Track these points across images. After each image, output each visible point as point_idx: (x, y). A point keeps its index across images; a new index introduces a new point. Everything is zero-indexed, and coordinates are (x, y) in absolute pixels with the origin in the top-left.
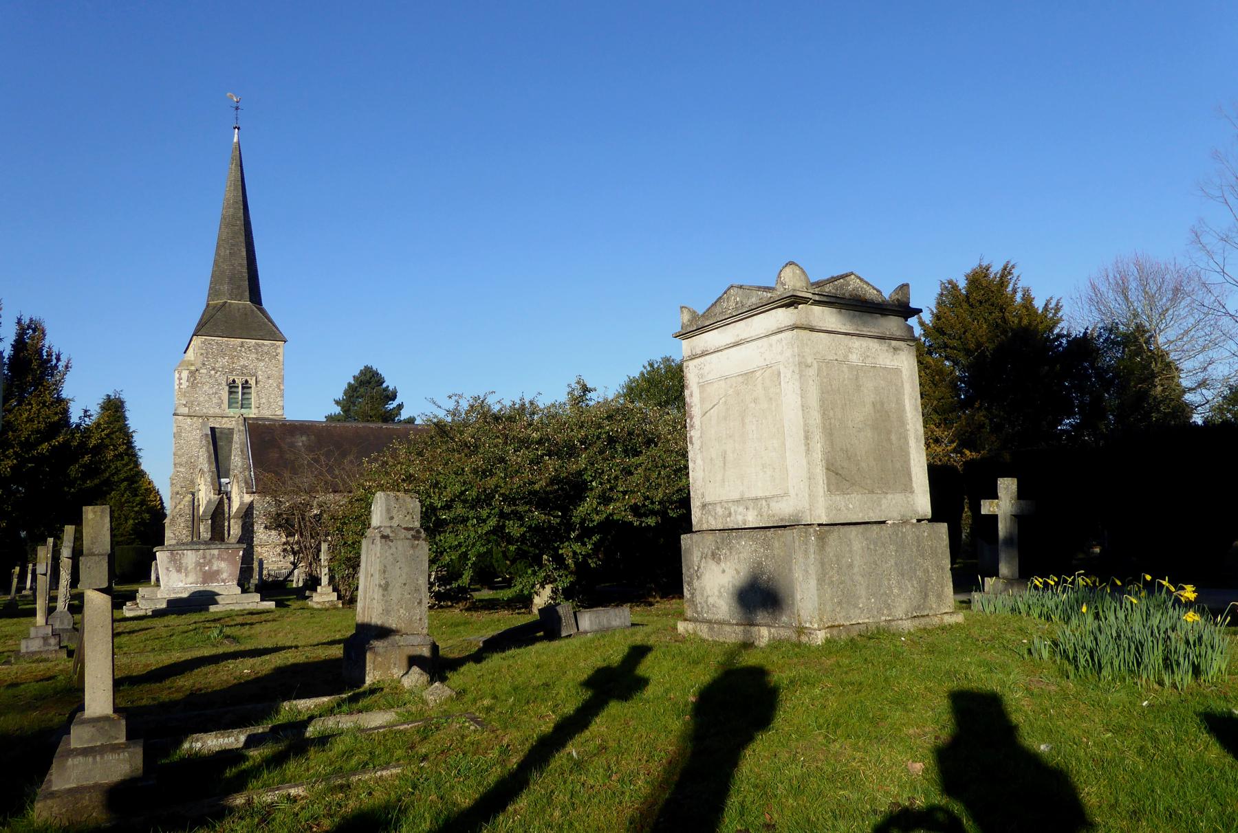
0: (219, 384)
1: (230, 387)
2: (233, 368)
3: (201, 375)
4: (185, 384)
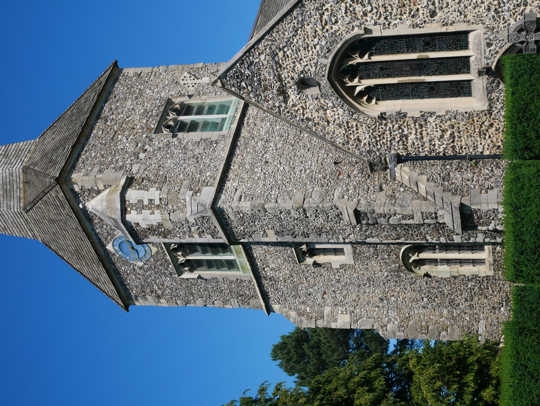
0: (168, 145)
2: (142, 128)
3: (141, 172)
4: (154, 194)
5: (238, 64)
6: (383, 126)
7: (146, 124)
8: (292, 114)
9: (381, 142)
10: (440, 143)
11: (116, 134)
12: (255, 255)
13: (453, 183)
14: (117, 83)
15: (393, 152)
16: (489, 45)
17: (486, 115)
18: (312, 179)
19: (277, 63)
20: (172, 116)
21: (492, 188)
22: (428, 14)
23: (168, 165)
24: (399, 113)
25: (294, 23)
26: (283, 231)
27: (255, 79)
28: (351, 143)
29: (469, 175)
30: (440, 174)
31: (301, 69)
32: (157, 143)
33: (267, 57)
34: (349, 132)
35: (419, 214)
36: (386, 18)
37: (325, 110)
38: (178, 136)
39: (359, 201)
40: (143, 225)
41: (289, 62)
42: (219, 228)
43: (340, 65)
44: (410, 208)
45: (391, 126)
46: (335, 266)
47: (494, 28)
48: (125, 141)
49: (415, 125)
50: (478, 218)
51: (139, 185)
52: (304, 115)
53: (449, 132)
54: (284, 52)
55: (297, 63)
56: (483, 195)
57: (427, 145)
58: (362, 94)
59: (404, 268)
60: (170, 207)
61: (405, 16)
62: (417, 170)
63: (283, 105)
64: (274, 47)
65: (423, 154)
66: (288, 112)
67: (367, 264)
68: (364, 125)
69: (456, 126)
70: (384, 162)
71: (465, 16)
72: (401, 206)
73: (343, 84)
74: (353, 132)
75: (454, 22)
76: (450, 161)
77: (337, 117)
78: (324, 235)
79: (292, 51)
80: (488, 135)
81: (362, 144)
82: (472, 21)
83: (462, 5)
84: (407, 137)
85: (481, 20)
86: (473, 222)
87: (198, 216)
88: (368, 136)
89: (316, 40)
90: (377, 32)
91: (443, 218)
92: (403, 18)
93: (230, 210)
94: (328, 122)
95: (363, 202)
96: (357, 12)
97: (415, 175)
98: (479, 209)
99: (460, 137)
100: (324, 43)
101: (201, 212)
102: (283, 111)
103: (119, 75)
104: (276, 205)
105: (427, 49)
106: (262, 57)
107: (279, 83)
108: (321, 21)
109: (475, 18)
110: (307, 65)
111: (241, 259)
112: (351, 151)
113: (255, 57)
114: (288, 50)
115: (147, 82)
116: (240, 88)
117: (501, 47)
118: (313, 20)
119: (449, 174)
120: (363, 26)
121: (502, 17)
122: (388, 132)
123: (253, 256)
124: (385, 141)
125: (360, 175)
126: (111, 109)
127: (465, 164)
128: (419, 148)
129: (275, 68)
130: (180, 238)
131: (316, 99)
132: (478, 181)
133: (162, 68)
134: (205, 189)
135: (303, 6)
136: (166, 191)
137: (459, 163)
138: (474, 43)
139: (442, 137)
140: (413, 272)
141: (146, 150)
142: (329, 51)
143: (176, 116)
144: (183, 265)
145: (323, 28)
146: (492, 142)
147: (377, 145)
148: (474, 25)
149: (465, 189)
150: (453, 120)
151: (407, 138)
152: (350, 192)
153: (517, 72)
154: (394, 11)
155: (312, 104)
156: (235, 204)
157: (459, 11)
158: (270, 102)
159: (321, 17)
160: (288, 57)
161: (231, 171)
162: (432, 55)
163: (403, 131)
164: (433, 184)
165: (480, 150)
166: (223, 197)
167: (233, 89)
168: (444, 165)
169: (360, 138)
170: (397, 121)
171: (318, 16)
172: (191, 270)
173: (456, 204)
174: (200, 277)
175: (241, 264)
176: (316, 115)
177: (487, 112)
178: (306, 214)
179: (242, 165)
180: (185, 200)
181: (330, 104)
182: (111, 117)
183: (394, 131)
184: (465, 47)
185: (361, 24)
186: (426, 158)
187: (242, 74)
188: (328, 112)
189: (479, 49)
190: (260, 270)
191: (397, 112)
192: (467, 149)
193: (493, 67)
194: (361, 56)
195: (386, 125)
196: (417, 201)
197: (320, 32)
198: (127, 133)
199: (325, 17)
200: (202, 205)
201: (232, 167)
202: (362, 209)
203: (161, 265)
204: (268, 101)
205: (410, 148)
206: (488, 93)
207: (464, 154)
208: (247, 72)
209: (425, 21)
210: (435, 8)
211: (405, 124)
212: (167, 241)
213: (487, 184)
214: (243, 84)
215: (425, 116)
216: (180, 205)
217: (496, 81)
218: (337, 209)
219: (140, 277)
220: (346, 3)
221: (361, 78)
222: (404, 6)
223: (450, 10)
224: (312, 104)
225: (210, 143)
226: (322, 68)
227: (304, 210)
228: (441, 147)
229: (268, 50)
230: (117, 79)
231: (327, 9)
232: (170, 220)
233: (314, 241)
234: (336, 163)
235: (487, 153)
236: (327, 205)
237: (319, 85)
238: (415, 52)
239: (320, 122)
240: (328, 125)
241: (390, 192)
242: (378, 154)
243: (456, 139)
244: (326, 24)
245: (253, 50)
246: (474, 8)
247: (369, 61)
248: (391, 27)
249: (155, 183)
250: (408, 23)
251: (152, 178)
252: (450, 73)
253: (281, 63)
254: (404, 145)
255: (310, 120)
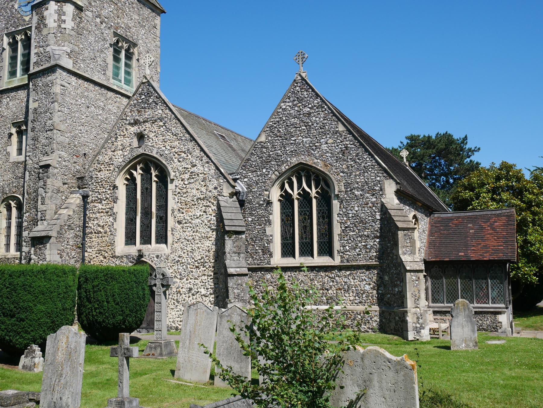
1: (115, 50)
2: (118, 23)
3: (86, 17)
4: (69, 24)
5: (157, 94)
6: (109, 187)
7: (121, 27)
8: (121, 127)
9: (98, 186)
10: (95, 224)
11: (115, 4)
12: (19, 92)
13: (66, 232)
14: (150, 11)
15: (90, 193)
16: (157, 257)
17: (112, 254)
18: (74, 137)
19: (156, 121)
20: (125, 46)
21: (61, 258)
22: (179, 220)
23: (90, 37)
24: (117, 198)
25: (180, 134)
26: (37, 113)
27: (146, 105)
28: (98, 165)
29: (71, 243)
30: (73, 223)
31: (151, 136)
32: (107, 32)
33: (160, 115)
34: (106, 165)
35: (45, 209)
36: (179, 193)
37: (122, 150)
38: (110, 48)
39: (57, 168)
40: (46, 13)
41: (156, 129)
42: (41, 68)
43: (151, 162)
44: (50, 203)
45: (108, 193)
46: (9, 149)
47: (168, 260)
48: (110, 10)
49: (108, 209)
50: (40, 248)
51: (77, 15)
52: (119, 135)
53: (102, 230)
54: (162, 126)
55: (154, 134)
56: (57, 251)
57: (94, 216)
58: (131, 175)
59: (5, 196)
60: (59, 35)
61: (180, 205)
62: (77, 209)
63: (127, 122)
64: (166, 119)
65: (87, 212)
66: (122, 125)
67: (9, 171)
68: (110, 175)
69: (106, 235)
70: (84, 187)
71: (176, 242)
72: (51, 197)
73: (139, 163)
74: (106, 168)
75: (173, 235)
76: (82, 230)
77: (117, 157)
78: (32, 142)
79: (163, 132)
80: (98, 255)
81: (97, 173)
82: (173, 246)
83: (184, 240)
84: (100, 203)
85: (173, 252)
86: (37, 244)
87: (51, 54)
88: (102, 177)
89: (169, 148)
90: (171, 187)
91: (41, 225)
92: (179, 203)
93: (54, 77)
94: (114, 151)
95: (56, 171)
96: (184, 175)
97: (73, 207)
98: (46, 248)
99: (98, 237)
100: (166, 152)
101: (54, 57)
102: (123, 122)
103: (156, 13)
104: (57, 111)
105: (158, 218)
106: (160, 111)
107: (142, 121)
108: (181, 152)
109: (175, 248)
110: (153, 140)
111: (16, 82)
112: (93, 165)
113: (161, 106)
114: (164, 129)
115: (150, 32)
116: (141, 94)
117: (155, 264)
118: (182, 146)
119: (73, 229)
120: (175, 178)
121: (174, 264)
122: (104, 190)
123: (19, 90)
124: (98, 188)
125: (76, 170)
126: (133, 3)
127: (79, 240)
128: (92, 210)
129: (153, 119)
130: (35, 39)
131: (130, 145)
132: (67, 248)
133: (158, 43)
134: (71, 61)
135: (191, 141)
136: (71, 34)
137: (80, 236)
138: (159, 248)
139: (99, 226)
140: (2, 203)
141: (102, 24)
142: (161, 155)
143: (125, 48)
144: (14, 38)
145: (176, 153)
146: (94, 258)
147: (96, 183)
148: (171, 248)
149: (61, 240)
150: (110, 233)
151: (99, 203)
152: (64, 163)
153: (138, 274)
154: (183, 198)
155: (127, 141)
156: (59, 81)
157: (180, 238)
158: (130, 114)
159: (183, 152)
160: (159, 128)
161: (83, 81)
162: (154, 221)
163: (104, 200)
164: (66, 218)
165: (88, 250)
166: (65, 74)
167: (140, 90)
168: (79, 226)
169: (102, 172)
170: (111, 197)
171: (184, 150)
172: (9, 44)
173: (50, 234)
174: (4, 49)
175: (13, 81)
176: (119, 143)
177: (114, 255)
178: (49, 131)
179: (87, 90)
180: (64, 46)
181: (126, 154)
182: (127, 3)
183: (105, 195)
184: (157, 242)
185: (176, 177)
186: (85, 215)
187: (150, 97)
188: (121, 152)
189: (155, 250)
190: (7, 94)
191: (117, 197)
192: (89, 242)
193: (143, 259)
194: (156, 176)
195: (109, 189)
196: (54, 208)
197: (174, 150)
198: (115, 12)
199: (183, 155)
200: (59, 58)
201: (86, 82)
202: (51, 170)
203: (15, 22)
204: (130, 112)
205: (92, 204)
206: (126, 256)
207: (86, 240)
208: (151, 100)
209: (175, 217)
210: (183, 224)
211: (109, 202)
212: (33, 29)
213: (65, 254)
214: (143, 97)
215: (113, 215)
216: (60, 42)
217: (134, 261)
218: (52, 153)
219: (6, 5)
220: (191, 168)
221: (142, 175)
222: (186, 205)
223: (181, 233)
224: (127, 141)
225: (104, 70)
226: (150, 150)
227: (52, 130)
228: (92, 225)
229: (165, 115)
230: (153, 11)
231: (188, 156)
232: (49, 33)
233: (28, 135)
234: (85, 154)
235: (86, 254)
236: (55, 146)
237: (139, 147)
238: (156, 211)
239: (114, 146)
240: (112, 151)
241: (62, 190)
242: (90, 183)
243: (97, 235)
244: (178, 155)
245: (165, 106)
246: (181, 248)
247: (153, 181)
248: (173, 196)
249: (78, 27)
250: (175, 207)
251: (81, 25)
252: (141, 232)
253: (155, 123)
254: (95, 200)
255: (116, 139)
